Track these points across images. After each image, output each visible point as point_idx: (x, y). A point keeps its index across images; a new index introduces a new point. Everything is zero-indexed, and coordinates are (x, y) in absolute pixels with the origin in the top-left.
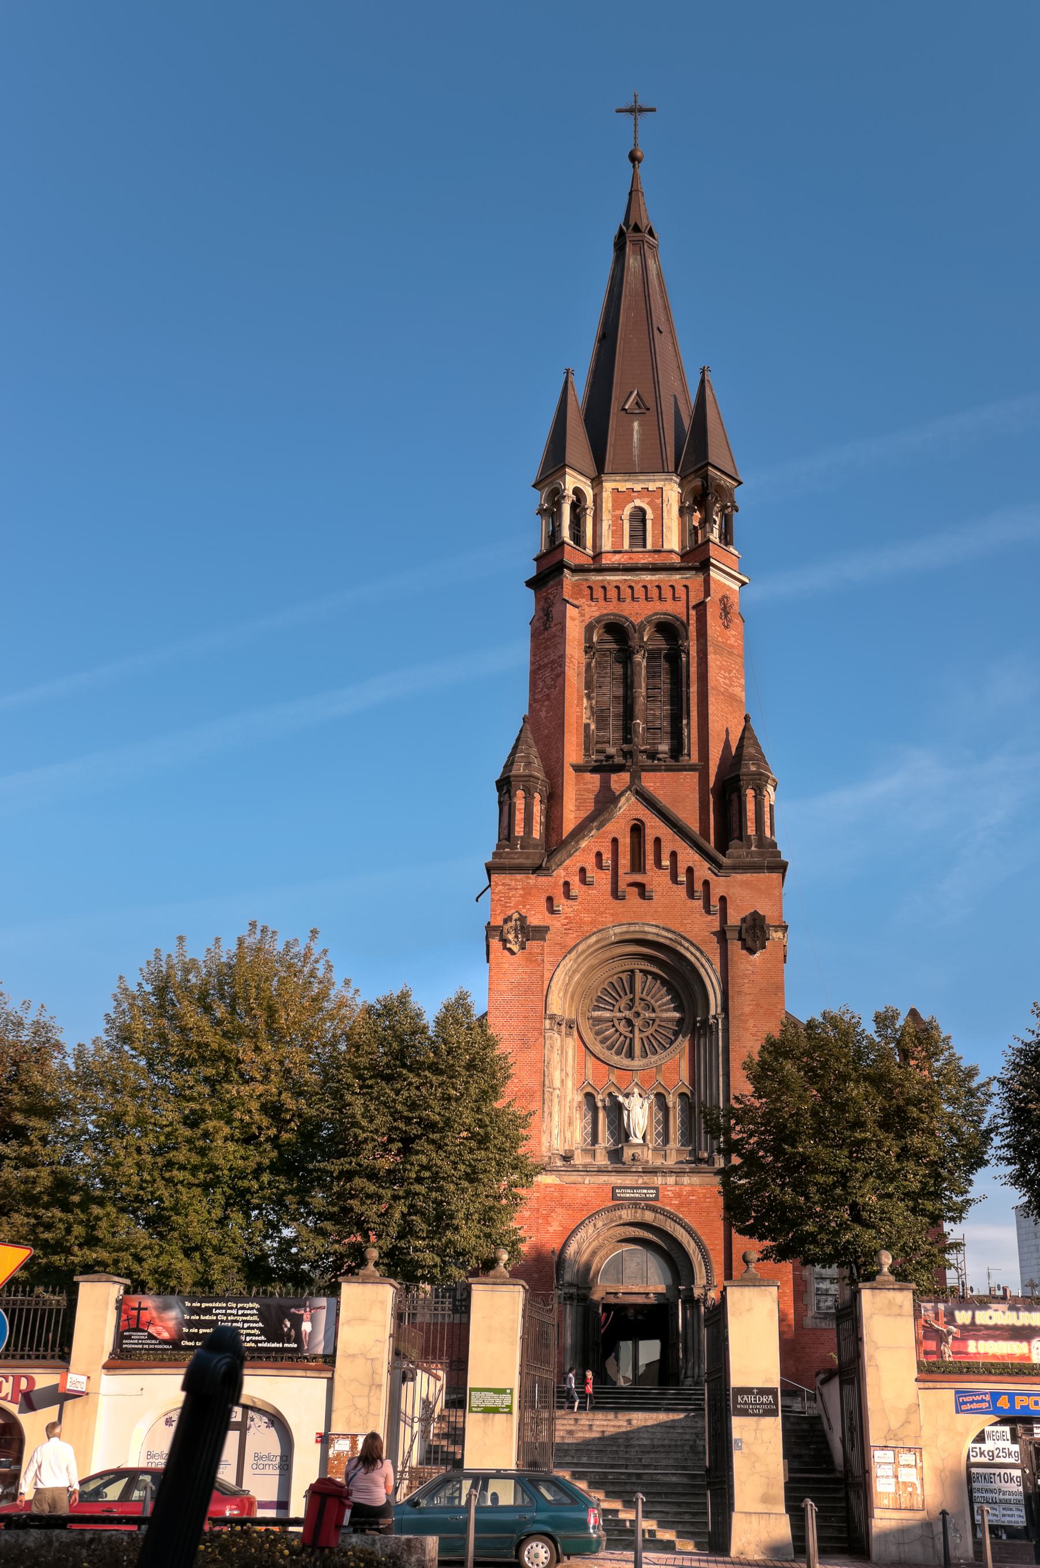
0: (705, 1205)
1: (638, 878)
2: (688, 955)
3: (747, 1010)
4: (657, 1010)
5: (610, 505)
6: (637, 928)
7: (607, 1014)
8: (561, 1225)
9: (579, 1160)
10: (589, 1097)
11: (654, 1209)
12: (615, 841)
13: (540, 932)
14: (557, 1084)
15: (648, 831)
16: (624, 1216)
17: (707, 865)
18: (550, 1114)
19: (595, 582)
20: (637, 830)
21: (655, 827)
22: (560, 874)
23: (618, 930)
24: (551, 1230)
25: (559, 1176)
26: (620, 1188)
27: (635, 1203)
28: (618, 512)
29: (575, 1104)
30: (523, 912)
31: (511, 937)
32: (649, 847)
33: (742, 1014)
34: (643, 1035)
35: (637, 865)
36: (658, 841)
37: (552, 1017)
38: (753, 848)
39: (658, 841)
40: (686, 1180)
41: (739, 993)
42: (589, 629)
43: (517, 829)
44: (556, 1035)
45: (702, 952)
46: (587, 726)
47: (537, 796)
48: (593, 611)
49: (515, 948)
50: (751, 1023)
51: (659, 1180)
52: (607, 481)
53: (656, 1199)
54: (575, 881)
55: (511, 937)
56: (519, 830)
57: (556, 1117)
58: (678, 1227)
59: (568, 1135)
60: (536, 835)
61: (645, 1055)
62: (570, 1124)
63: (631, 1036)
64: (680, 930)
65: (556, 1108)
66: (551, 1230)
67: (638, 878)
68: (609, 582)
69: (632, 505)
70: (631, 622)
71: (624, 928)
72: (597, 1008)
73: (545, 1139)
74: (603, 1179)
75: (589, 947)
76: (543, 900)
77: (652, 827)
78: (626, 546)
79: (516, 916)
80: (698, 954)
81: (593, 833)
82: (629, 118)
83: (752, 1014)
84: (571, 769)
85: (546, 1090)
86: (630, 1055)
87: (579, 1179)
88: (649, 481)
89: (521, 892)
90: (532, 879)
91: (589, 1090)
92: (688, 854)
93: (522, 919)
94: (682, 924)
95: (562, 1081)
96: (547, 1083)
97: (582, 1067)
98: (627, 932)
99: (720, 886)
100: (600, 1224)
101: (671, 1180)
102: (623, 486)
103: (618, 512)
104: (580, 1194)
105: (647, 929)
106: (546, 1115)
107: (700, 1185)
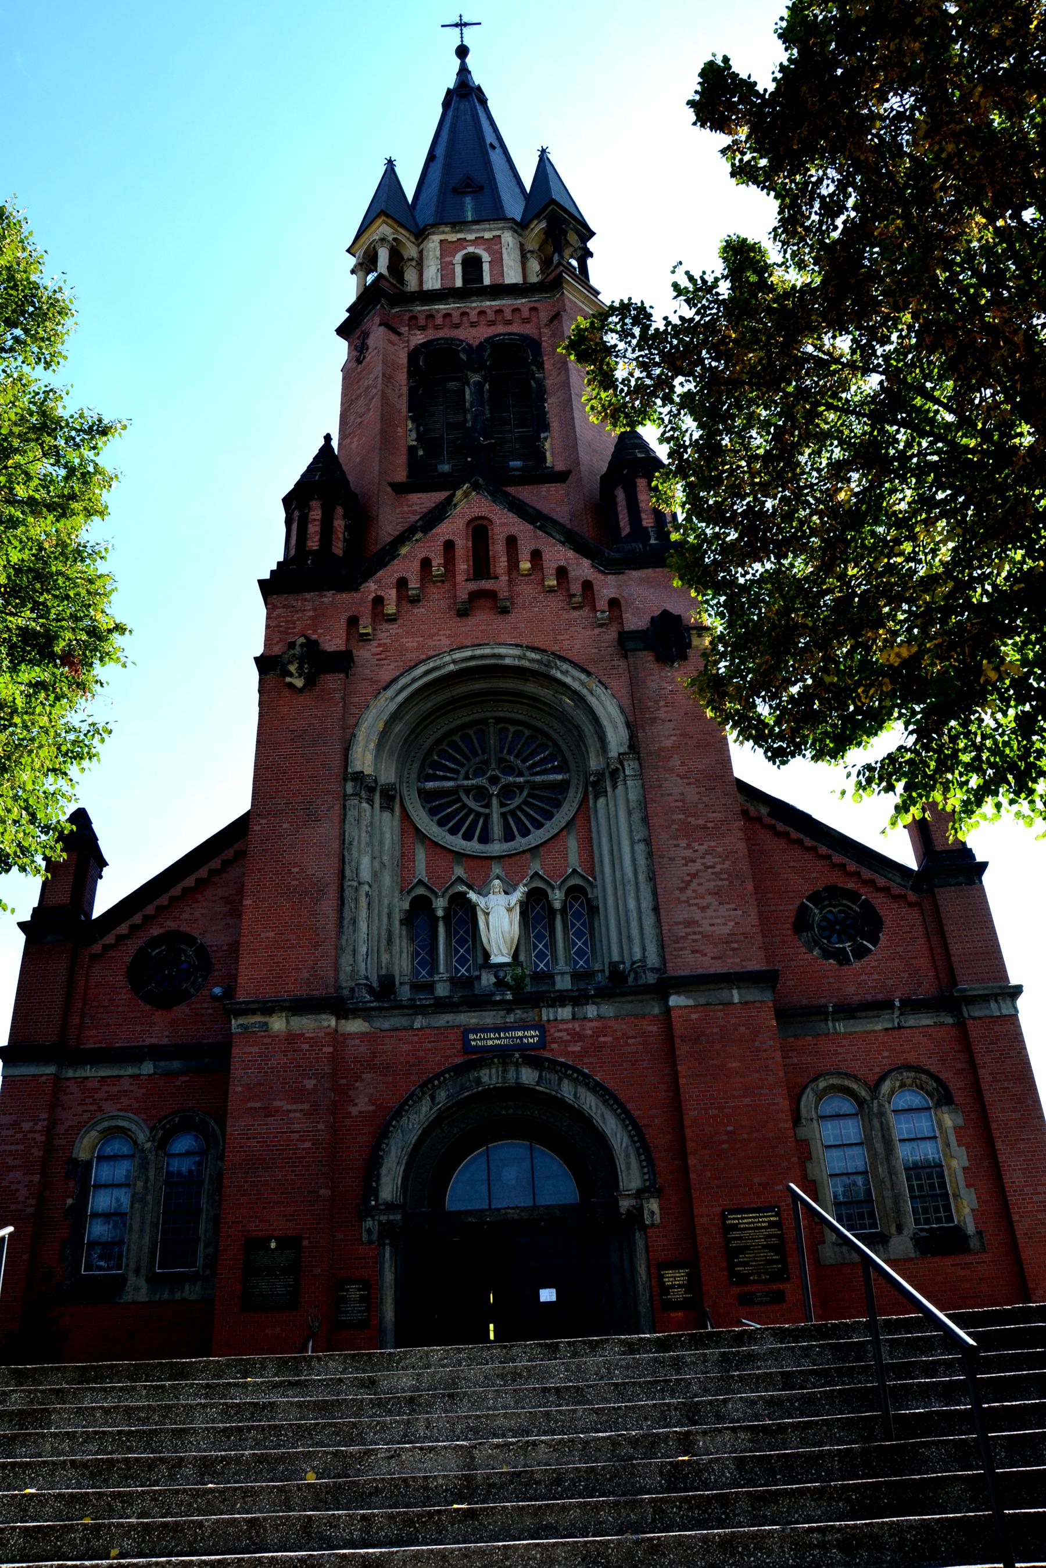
0: (629, 1049)
1: (486, 584)
2: (568, 680)
4: (526, 772)
5: (438, 253)
6: (487, 651)
7: (451, 784)
8: (371, 1102)
9: (405, 993)
10: (420, 908)
11: (535, 1062)
12: (449, 546)
14: (366, 875)
15: (497, 530)
16: (485, 1079)
17: (586, 563)
18: (354, 921)
19: (419, 312)
21: (504, 523)
22: (371, 588)
23: (458, 656)
24: (354, 1111)
25: (366, 1019)
26: (475, 1031)
27: (503, 1055)
28: (448, 259)
29: (397, 916)
30: (314, 637)
31: (292, 668)
32: (498, 549)
33: (662, 749)
34: (503, 810)
35: (482, 567)
36: (512, 542)
38: (652, 541)
39: (512, 542)
40: (591, 1011)
41: (654, 720)
42: (414, 355)
43: (310, 544)
44: (365, 805)
45: (589, 674)
46: (412, 450)
48: (419, 338)
49: (299, 683)
50: (676, 761)
52: (433, 233)
53: (542, 1044)
54: (391, 595)
56: (313, 544)
57: (363, 926)
58: (582, 1091)
59: (385, 957)
60: (338, 548)
61: (508, 837)
62: (390, 941)
63: (487, 811)
64: (555, 648)
65: (363, 914)
66: (354, 1111)
67: (486, 584)
68: (438, 311)
69: (465, 252)
70: (467, 344)
71: (468, 653)
73: (346, 960)
74: (443, 1020)
75: (414, 680)
76: (343, 622)
77: (502, 525)
78: (459, 283)
79: (302, 640)
80: (583, 677)
81: (417, 537)
82: (458, 30)
83: (676, 747)
84: (389, 489)
85: (347, 883)
87: (403, 1022)
88: (484, 230)
89: (311, 613)
91: (421, 891)
92: (558, 551)
93: (312, 645)
94: (556, 641)
95: (375, 874)
96: (348, 873)
98: (472, 658)
99: (608, 587)
100: (442, 1095)
101: (565, 1013)
102: (453, 237)
103: (448, 259)
104: (406, 1047)
105: (503, 651)
106: (346, 922)
107: (616, 1018)
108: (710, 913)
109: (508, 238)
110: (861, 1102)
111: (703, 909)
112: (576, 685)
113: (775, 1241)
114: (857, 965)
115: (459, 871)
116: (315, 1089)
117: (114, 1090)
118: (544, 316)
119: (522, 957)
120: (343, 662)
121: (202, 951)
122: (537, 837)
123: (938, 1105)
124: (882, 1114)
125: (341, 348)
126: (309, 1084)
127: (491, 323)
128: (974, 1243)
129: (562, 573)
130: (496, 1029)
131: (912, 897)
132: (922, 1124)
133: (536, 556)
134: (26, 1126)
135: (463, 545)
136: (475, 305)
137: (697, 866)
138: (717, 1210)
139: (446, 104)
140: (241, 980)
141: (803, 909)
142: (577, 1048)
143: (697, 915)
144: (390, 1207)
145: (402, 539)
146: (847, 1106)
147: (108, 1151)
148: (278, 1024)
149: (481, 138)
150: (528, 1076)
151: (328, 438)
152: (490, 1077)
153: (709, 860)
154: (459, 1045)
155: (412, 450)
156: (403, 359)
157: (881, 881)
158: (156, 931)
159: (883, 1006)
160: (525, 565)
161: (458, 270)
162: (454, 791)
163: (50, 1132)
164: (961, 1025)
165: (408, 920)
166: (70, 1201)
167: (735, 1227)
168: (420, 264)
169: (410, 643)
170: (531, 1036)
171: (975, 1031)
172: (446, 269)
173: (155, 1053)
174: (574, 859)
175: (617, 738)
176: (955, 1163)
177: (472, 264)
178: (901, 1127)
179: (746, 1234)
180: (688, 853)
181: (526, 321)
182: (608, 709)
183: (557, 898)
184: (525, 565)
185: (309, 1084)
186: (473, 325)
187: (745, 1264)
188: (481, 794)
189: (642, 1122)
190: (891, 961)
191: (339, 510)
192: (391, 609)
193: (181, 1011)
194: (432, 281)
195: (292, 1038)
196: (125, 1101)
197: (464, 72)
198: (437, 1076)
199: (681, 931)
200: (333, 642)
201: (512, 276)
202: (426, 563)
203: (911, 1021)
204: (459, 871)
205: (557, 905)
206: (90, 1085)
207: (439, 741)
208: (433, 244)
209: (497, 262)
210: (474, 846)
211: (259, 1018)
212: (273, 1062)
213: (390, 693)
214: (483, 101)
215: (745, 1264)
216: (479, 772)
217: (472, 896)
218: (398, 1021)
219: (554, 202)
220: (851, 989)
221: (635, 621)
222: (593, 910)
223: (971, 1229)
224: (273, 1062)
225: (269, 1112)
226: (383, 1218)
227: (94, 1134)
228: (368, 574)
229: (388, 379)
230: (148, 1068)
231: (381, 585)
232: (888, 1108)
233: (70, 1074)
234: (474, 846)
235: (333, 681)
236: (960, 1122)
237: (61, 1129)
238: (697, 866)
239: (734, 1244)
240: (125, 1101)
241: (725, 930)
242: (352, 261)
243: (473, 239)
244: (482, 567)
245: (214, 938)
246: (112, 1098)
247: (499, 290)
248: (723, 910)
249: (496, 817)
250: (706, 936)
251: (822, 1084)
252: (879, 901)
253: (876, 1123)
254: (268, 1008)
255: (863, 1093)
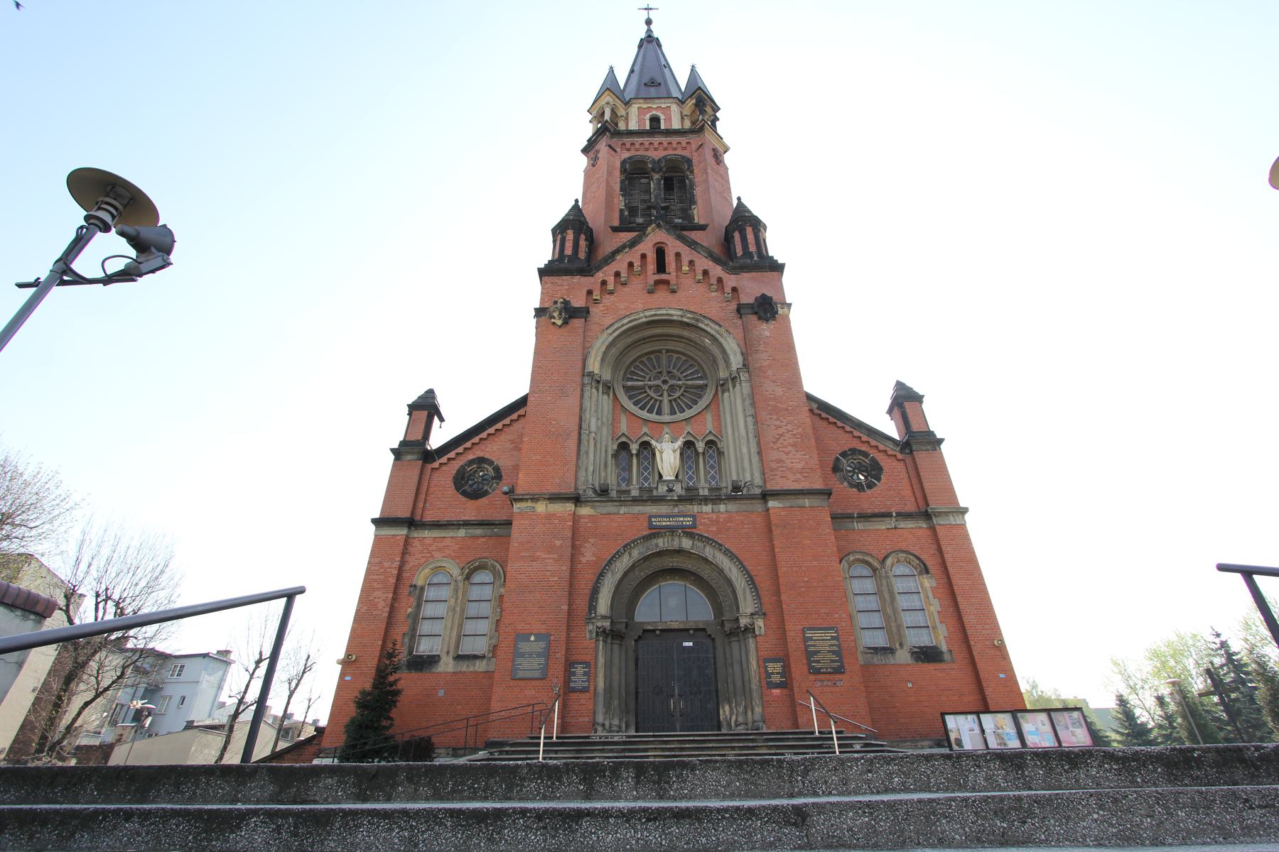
2: (708, 329)
3: (766, 364)
9: (614, 494)
11: (691, 536)
12: (644, 256)
13: (584, 313)
14: (593, 428)
16: (661, 545)
17: (719, 268)
18: (587, 453)
20: (660, 253)
21: (673, 245)
22: (600, 276)
23: (647, 313)
24: (584, 560)
25: (593, 507)
26: (655, 517)
27: (672, 530)
29: (610, 452)
32: (670, 259)
35: (661, 267)
36: (678, 255)
37: (591, 374)
39: (678, 255)
40: (722, 507)
41: (757, 351)
42: (623, 163)
46: (621, 211)
47: (583, 237)
48: (626, 155)
50: (770, 373)
51: (695, 508)
55: (556, 314)
57: (591, 455)
59: (603, 474)
61: (673, 412)
66: (584, 560)
67: (663, 276)
72: (629, 379)
73: (582, 473)
74: (637, 509)
76: (584, 292)
78: (648, 127)
86: (659, 413)
90: (577, 279)
91: (623, 439)
93: (566, 303)
95: (598, 428)
97: (615, 422)
99: (731, 281)
101: (707, 508)
102: (645, 106)
104: (615, 525)
108: (791, 456)
109: (675, 108)
110: (875, 570)
111: (787, 454)
112: (713, 332)
113: (835, 648)
114: (869, 492)
115: (645, 430)
116: (561, 546)
117: (441, 545)
118: (694, 146)
119: (680, 477)
120: (584, 313)
121: (497, 469)
122: (688, 413)
123: (920, 573)
124: (888, 577)
125: (583, 161)
126: (558, 543)
127: (665, 149)
128: (947, 657)
129: (705, 273)
130: (669, 516)
131: (900, 456)
132: (910, 584)
133: (691, 263)
134: (386, 564)
135: (652, 256)
136: (656, 140)
137: (783, 430)
138: (800, 627)
139: (640, 46)
140: (520, 482)
141: (837, 459)
142: (714, 529)
143: (784, 457)
144: (604, 617)
145: (618, 251)
146: (866, 571)
147: (435, 581)
148: (541, 507)
149: (659, 61)
150: (686, 543)
151: (577, 201)
152: (662, 543)
153: (789, 427)
154: (646, 524)
155: (621, 211)
156: (618, 165)
157: (881, 447)
158: (471, 457)
159: (889, 515)
160: (685, 268)
161: (648, 123)
162: (642, 388)
163: (400, 569)
164: (933, 529)
165: (616, 456)
166: (410, 610)
167: (811, 639)
168: (627, 119)
169: (621, 306)
170: (688, 521)
171: (941, 532)
172: (640, 121)
173: (467, 524)
174: (710, 426)
175: (736, 361)
176: (932, 608)
177: (654, 120)
178: (899, 585)
179: (817, 643)
180: (778, 423)
181: (684, 149)
182: (732, 346)
183: (700, 446)
184: (685, 268)
185: (558, 543)
186: (656, 149)
187: (818, 662)
188: (657, 388)
189: (753, 573)
190: (893, 488)
191: (583, 237)
192: (610, 287)
193: (483, 501)
194: (633, 126)
195: (549, 516)
196: (447, 552)
197: (649, 30)
198: (633, 542)
199: (774, 465)
200: (578, 302)
201: (676, 125)
202: (631, 265)
203: (902, 525)
204: (645, 430)
205: (700, 450)
206: (427, 541)
207: (635, 360)
208: (634, 109)
209: (669, 119)
210: (653, 417)
211: (529, 504)
212: (537, 530)
213: (610, 331)
214: (660, 46)
215: (818, 662)
216: (656, 378)
217: (653, 443)
218: (610, 508)
219: (700, 88)
220: (866, 506)
221: (748, 298)
222: (720, 453)
223: (944, 648)
224: (537, 530)
225: (534, 559)
226: (599, 624)
227: (427, 570)
228: (599, 268)
229: (610, 173)
230: (462, 533)
231: (606, 274)
232: (891, 574)
233: (416, 535)
234: (653, 417)
235: (577, 323)
236: (934, 584)
237: (407, 567)
238: (783, 430)
239: (811, 649)
240: (447, 552)
241: (800, 466)
242: (590, 117)
243: (656, 108)
244: (661, 267)
245: (503, 462)
246: (439, 549)
247: (670, 133)
248: (798, 455)
249: (666, 402)
250: (790, 469)
251: (852, 558)
252: (880, 458)
253: (884, 582)
254: (535, 499)
255: (876, 564)
